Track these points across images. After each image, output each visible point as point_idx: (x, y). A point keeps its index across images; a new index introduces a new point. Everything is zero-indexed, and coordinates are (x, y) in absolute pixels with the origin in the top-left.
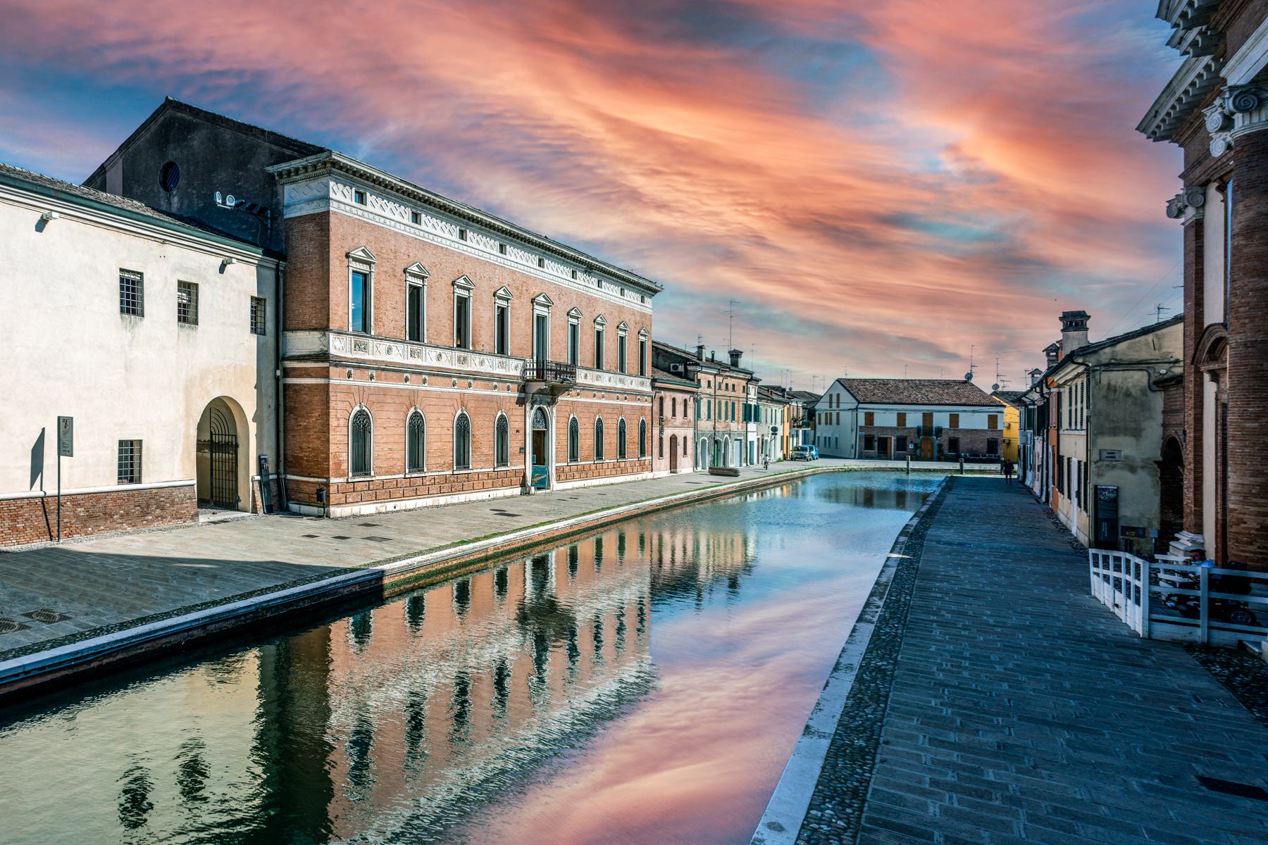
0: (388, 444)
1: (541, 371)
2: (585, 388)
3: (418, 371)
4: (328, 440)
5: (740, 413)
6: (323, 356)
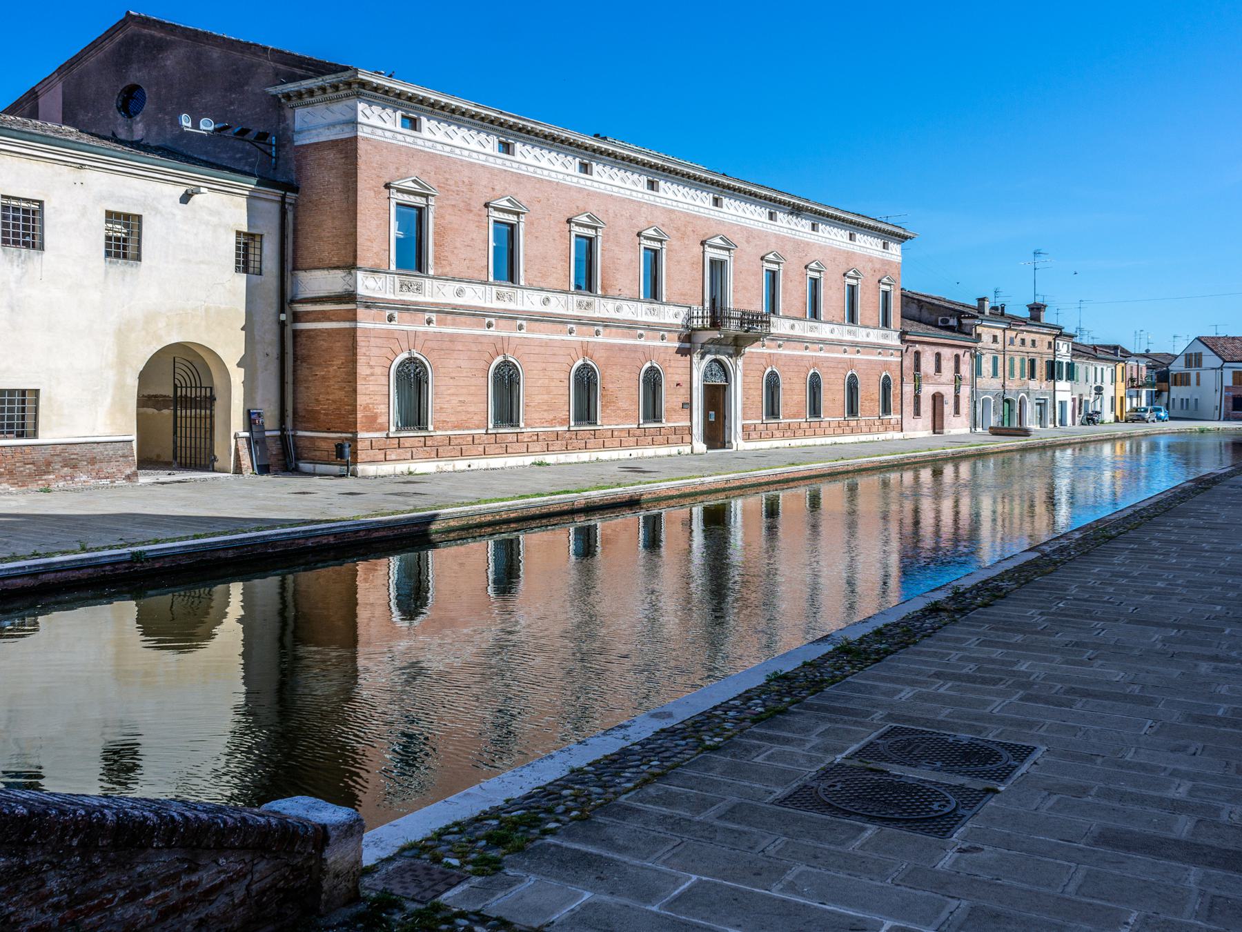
0: (458, 396)
1: (717, 317)
2: (789, 339)
3: (511, 316)
4: (355, 391)
5: (1041, 369)
6: (350, 297)
